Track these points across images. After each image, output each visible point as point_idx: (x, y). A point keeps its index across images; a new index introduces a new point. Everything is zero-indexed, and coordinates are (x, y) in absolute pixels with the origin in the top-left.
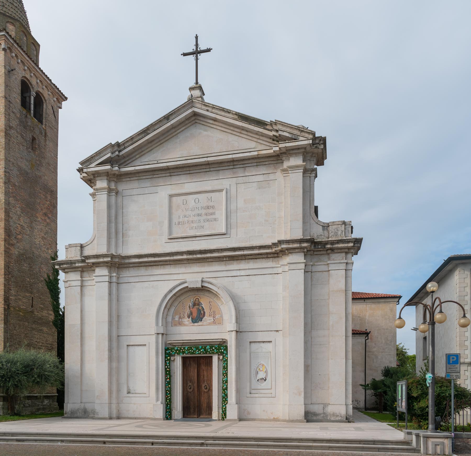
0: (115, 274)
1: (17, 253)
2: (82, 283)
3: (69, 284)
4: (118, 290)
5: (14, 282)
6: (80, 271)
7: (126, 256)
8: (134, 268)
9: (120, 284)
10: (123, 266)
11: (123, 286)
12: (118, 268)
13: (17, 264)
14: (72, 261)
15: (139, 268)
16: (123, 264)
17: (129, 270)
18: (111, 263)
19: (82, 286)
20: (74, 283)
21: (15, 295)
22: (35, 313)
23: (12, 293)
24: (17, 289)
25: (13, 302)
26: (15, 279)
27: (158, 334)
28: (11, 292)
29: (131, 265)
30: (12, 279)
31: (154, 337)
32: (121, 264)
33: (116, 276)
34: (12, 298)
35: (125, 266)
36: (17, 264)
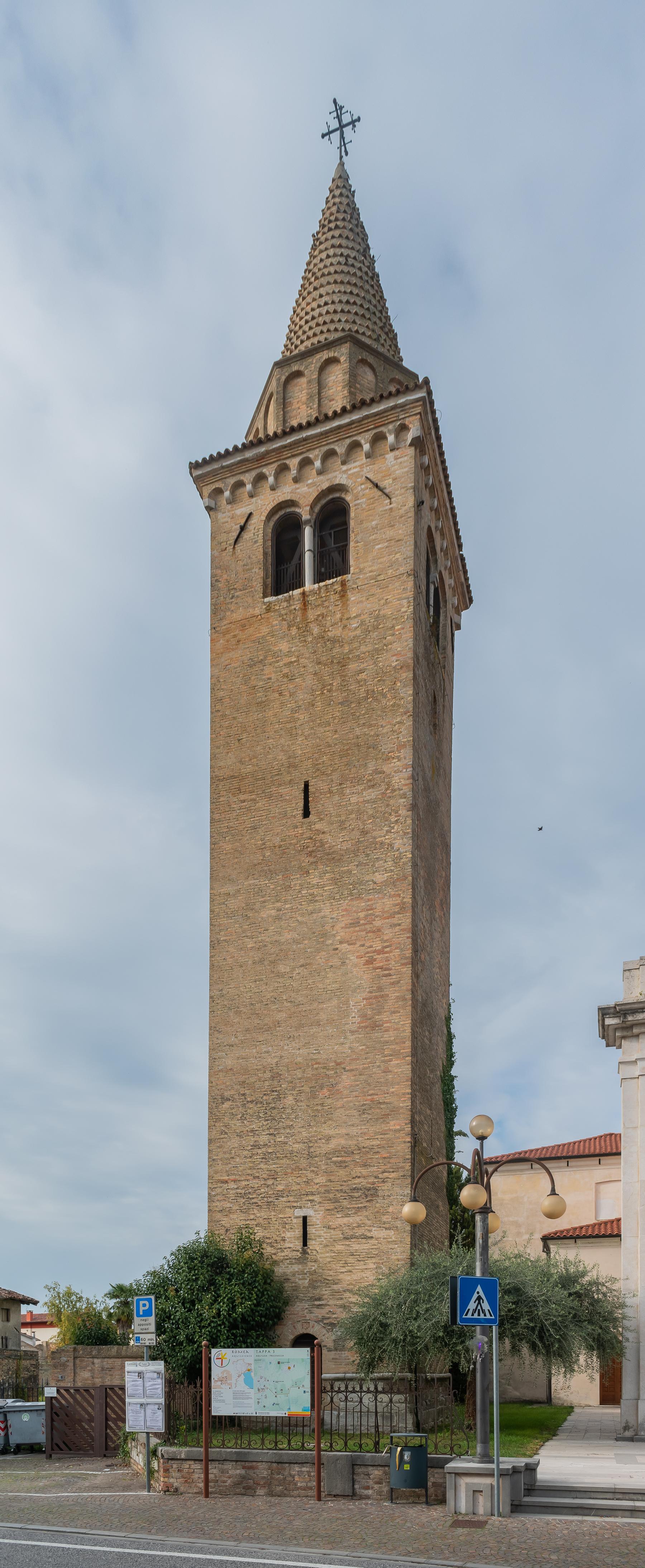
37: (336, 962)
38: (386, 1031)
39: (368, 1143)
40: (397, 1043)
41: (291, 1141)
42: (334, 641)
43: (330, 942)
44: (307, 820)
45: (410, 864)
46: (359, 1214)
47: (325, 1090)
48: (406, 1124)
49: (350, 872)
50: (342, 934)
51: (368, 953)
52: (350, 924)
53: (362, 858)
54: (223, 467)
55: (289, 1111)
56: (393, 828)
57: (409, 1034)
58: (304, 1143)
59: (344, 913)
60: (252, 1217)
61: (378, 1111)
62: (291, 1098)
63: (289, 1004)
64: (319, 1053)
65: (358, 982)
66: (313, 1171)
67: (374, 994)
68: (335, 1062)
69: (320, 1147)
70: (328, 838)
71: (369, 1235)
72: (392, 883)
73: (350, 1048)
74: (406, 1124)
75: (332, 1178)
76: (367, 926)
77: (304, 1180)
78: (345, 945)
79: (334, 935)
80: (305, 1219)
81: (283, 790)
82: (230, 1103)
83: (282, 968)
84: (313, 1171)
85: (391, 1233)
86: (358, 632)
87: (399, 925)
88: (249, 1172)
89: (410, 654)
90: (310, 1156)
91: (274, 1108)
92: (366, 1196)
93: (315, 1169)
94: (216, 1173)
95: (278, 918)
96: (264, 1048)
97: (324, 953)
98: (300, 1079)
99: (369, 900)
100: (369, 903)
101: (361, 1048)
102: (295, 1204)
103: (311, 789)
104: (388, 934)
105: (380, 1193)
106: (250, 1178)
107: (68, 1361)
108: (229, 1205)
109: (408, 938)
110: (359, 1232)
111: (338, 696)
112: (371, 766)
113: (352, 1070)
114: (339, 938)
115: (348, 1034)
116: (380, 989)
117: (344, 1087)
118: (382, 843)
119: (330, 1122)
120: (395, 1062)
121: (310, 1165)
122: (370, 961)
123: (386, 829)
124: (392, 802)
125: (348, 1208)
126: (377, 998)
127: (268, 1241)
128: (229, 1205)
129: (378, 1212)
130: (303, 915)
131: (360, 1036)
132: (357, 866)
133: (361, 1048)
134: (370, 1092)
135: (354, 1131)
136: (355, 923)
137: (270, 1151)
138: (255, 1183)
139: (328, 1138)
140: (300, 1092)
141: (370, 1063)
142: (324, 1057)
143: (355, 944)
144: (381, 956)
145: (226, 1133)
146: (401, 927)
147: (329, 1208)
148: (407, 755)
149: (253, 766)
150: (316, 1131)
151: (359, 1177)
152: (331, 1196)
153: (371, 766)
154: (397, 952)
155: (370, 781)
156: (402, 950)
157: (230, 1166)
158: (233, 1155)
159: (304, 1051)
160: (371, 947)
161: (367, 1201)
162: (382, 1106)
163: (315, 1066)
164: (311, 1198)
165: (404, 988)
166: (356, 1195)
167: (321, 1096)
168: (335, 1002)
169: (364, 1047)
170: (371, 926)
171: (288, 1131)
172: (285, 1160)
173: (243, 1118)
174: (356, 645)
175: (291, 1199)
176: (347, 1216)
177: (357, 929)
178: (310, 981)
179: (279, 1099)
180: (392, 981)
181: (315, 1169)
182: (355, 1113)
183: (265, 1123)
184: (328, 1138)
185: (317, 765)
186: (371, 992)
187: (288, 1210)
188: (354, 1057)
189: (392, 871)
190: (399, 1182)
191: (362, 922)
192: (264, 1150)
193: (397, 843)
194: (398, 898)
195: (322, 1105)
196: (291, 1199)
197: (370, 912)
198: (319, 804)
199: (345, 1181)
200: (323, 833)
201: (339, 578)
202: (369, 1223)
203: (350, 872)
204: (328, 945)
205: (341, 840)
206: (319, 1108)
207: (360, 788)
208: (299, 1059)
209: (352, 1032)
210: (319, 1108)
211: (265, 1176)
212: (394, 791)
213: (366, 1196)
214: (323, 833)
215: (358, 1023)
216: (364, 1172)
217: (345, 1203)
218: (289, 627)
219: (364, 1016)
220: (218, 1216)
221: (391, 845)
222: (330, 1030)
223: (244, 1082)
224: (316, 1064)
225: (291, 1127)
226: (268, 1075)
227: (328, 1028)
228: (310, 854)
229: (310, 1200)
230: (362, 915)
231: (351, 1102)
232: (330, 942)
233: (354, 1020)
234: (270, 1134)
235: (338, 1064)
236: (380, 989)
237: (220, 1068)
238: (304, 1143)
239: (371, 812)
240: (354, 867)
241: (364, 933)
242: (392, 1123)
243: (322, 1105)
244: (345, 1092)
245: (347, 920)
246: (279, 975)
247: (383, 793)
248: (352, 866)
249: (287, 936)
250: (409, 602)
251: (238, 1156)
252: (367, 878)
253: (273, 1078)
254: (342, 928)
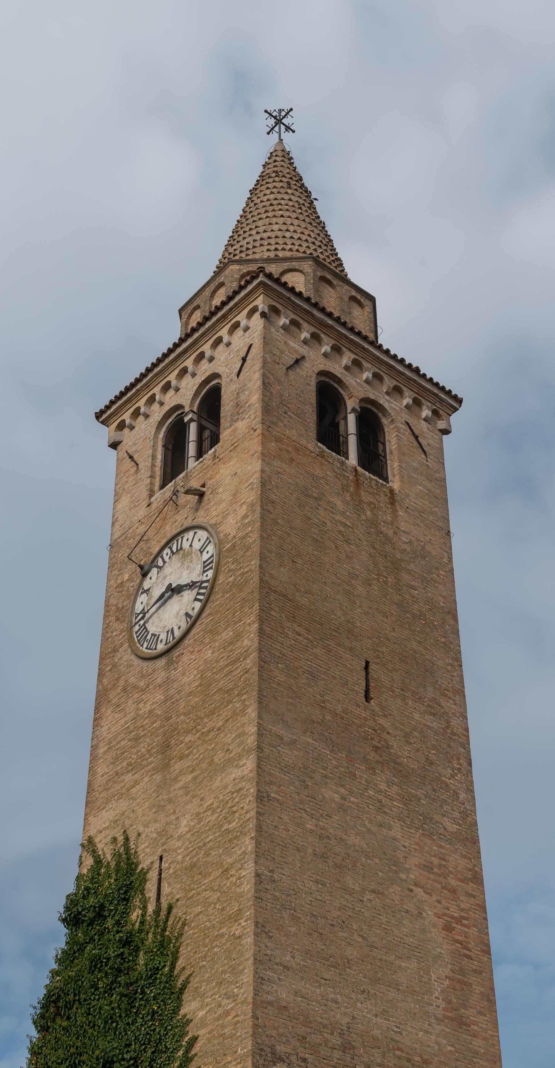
40: (488, 1060)
52: (424, 865)
65: (438, 950)
83: (349, 881)
100: (442, 850)
130: (371, 821)
131: (447, 1030)
133: (449, 1048)
169: (452, 1049)
178: (384, 919)
180: (474, 967)
188: (443, 1059)
200: (388, 733)
208: (376, 1032)
215: (444, 1009)
226: (336, 1040)
227: (409, 1000)
237: (270, 998)
239: (434, 743)
248: (419, 793)
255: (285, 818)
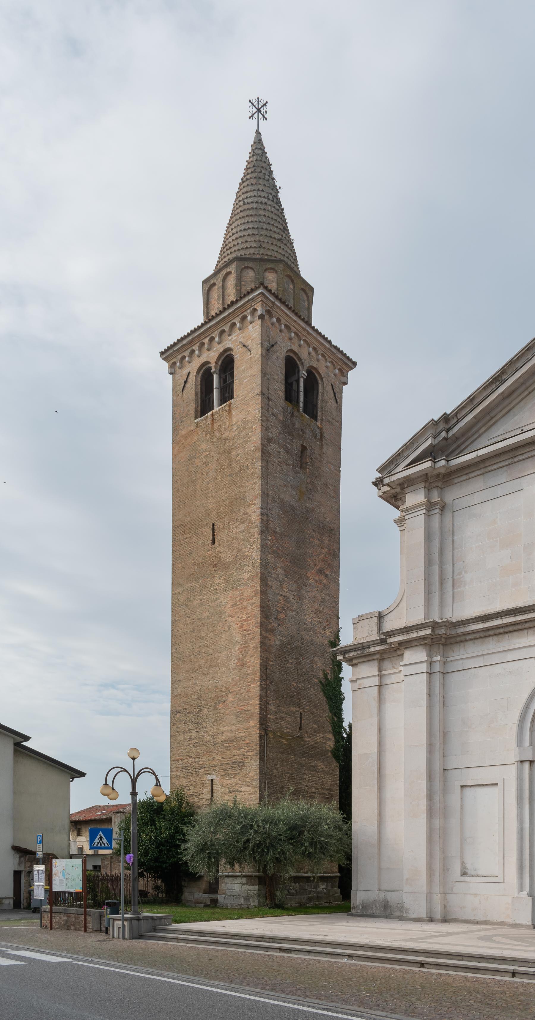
0: (438, 658)
1: (278, 643)
2: (380, 681)
3: (360, 684)
4: (444, 685)
5: (274, 690)
6: (377, 659)
7: (459, 621)
8: (476, 641)
9: (448, 674)
10: (453, 640)
11: (454, 678)
12: (444, 645)
13: (278, 662)
14: (364, 645)
15: (484, 639)
16: (454, 637)
17: (464, 646)
18: (432, 637)
19: (380, 686)
20: (367, 683)
21: (276, 712)
22: (305, 739)
23: (271, 710)
24: (278, 702)
25: (273, 724)
26: (276, 685)
27: (522, 762)
28: (270, 707)
29: (469, 637)
30: (271, 686)
31: (514, 769)
32: (451, 638)
33: (440, 661)
34: (271, 717)
35: (458, 639)
36: (278, 662)
37: (226, 628)
38: (249, 667)
39: (240, 735)
40: (253, 674)
41: (206, 735)
42: (226, 439)
43: (224, 616)
44: (214, 546)
45: (260, 567)
46: (236, 777)
47: (221, 704)
48: (257, 723)
49: (232, 574)
50: (229, 611)
51: (240, 621)
53: (238, 565)
54: (174, 351)
55: (205, 717)
56: (252, 546)
57: (259, 669)
58: (212, 736)
59: (230, 599)
60: (189, 780)
61: (245, 715)
62: (206, 710)
63: (205, 655)
64: (218, 682)
66: (215, 753)
67: (243, 646)
68: (226, 687)
69: (219, 738)
70: (223, 555)
71: (240, 790)
72: (251, 579)
73: (232, 679)
74: (257, 723)
75: (224, 756)
76: (240, 606)
77: (212, 758)
78: (230, 617)
79: (225, 612)
80: (212, 780)
81: (204, 530)
82: (179, 714)
83: (203, 634)
84: (215, 753)
85: (250, 788)
86: (236, 433)
87: (255, 603)
88: (188, 754)
89: (260, 442)
90: (215, 744)
91: (198, 716)
92: (239, 767)
93: (216, 751)
94: (173, 755)
95: (201, 605)
96: (194, 681)
97: (221, 623)
98: (210, 698)
99: (241, 590)
100: (241, 592)
101: (237, 678)
102: (208, 773)
103: (216, 528)
104: (250, 609)
105: (245, 765)
106: (188, 757)
107: (108, 864)
108: (179, 774)
109: (258, 611)
110: (236, 788)
111: (227, 471)
112: (242, 511)
113: (233, 692)
114: (227, 614)
115: (232, 670)
116: (246, 642)
117: (229, 702)
118: (247, 556)
119: (223, 723)
120: (252, 686)
121: (214, 749)
122: (241, 627)
123: (249, 547)
124: (251, 531)
125: (231, 774)
126: (245, 648)
127: (196, 794)
128: (179, 774)
129: (244, 776)
130: (211, 602)
132: (236, 570)
134: (241, 704)
135: (234, 728)
136: (235, 605)
137: (197, 741)
138: (190, 761)
139: (222, 733)
140: (210, 706)
141: (241, 687)
142: (221, 684)
143: (234, 617)
144: (246, 623)
145: (178, 732)
146: (256, 605)
147: (222, 774)
148: (258, 501)
149: (190, 517)
150: (217, 729)
151: (236, 755)
152: (223, 767)
153: (242, 511)
154: (253, 620)
155: (241, 519)
156: (256, 618)
157: (180, 751)
158: (181, 745)
159: (212, 682)
160: (242, 618)
161: (240, 770)
162: (247, 712)
163: (217, 690)
164: (214, 768)
165: (256, 641)
166: (235, 766)
167: (219, 708)
168: (225, 652)
170: (242, 605)
171: (205, 729)
172: (203, 746)
173: (185, 723)
174: (236, 440)
175: (206, 769)
176: (230, 778)
177: (236, 607)
179: (201, 710)
180: (251, 637)
181: (216, 751)
182: (234, 717)
183: (195, 725)
184: (222, 733)
185: (218, 513)
186: (241, 645)
187: (204, 776)
188: (234, 684)
189: (251, 571)
190: (253, 757)
191: (238, 603)
192: (194, 741)
193: (254, 555)
194: (254, 588)
195: (220, 713)
196: (206, 769)
197: (242, 597)
198: (221, 536)
199: (229, 758)
200: (221, 552)
201: (227, 403)
202: (240, 782)
203: (232, 574)
204: (222, 619)
205: (229, 556)
206: (218, 715)
207: (237, 524)
208: (210, 687)
209: (233, 669)
210: (218, 715)
211: (194, 756)
212: (252, 524)
213: (239, 767)
214: (221, 552)
216: (238, 752)
217: (230, 771)
218: (206, 434)
219: (238, 659)
220: (174, 780)
221: (251, 556)
222: (224, 669)
223: (186, 702)
224: (217, 689)
225: (206, 727)
226: (196, 697)
228: (215, 566)
229: (214, 770)
230: (238, 599)
231: (232, 710)
232: (224, 616)
233: (234, 662)
234: (197, 732)
235: (227, 688)
236: (246, 642)
237: (176, 694)
238: (212, 736)
240: (235, 571)
241: (238, 610)
242: (251, 722)
243: (220, 713)
244: (230, 705)
245: (231, 603)
246: (201, 638)
247: (248, 526)
248: (234, 571)
249: (205, 615)
250: (259, 411)
251: (183, 745)
252: (240, 577)
253: (198, 699)
254: (229, 608)
255: (181, 625)
